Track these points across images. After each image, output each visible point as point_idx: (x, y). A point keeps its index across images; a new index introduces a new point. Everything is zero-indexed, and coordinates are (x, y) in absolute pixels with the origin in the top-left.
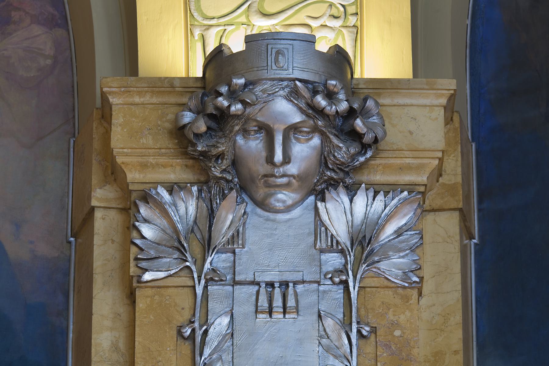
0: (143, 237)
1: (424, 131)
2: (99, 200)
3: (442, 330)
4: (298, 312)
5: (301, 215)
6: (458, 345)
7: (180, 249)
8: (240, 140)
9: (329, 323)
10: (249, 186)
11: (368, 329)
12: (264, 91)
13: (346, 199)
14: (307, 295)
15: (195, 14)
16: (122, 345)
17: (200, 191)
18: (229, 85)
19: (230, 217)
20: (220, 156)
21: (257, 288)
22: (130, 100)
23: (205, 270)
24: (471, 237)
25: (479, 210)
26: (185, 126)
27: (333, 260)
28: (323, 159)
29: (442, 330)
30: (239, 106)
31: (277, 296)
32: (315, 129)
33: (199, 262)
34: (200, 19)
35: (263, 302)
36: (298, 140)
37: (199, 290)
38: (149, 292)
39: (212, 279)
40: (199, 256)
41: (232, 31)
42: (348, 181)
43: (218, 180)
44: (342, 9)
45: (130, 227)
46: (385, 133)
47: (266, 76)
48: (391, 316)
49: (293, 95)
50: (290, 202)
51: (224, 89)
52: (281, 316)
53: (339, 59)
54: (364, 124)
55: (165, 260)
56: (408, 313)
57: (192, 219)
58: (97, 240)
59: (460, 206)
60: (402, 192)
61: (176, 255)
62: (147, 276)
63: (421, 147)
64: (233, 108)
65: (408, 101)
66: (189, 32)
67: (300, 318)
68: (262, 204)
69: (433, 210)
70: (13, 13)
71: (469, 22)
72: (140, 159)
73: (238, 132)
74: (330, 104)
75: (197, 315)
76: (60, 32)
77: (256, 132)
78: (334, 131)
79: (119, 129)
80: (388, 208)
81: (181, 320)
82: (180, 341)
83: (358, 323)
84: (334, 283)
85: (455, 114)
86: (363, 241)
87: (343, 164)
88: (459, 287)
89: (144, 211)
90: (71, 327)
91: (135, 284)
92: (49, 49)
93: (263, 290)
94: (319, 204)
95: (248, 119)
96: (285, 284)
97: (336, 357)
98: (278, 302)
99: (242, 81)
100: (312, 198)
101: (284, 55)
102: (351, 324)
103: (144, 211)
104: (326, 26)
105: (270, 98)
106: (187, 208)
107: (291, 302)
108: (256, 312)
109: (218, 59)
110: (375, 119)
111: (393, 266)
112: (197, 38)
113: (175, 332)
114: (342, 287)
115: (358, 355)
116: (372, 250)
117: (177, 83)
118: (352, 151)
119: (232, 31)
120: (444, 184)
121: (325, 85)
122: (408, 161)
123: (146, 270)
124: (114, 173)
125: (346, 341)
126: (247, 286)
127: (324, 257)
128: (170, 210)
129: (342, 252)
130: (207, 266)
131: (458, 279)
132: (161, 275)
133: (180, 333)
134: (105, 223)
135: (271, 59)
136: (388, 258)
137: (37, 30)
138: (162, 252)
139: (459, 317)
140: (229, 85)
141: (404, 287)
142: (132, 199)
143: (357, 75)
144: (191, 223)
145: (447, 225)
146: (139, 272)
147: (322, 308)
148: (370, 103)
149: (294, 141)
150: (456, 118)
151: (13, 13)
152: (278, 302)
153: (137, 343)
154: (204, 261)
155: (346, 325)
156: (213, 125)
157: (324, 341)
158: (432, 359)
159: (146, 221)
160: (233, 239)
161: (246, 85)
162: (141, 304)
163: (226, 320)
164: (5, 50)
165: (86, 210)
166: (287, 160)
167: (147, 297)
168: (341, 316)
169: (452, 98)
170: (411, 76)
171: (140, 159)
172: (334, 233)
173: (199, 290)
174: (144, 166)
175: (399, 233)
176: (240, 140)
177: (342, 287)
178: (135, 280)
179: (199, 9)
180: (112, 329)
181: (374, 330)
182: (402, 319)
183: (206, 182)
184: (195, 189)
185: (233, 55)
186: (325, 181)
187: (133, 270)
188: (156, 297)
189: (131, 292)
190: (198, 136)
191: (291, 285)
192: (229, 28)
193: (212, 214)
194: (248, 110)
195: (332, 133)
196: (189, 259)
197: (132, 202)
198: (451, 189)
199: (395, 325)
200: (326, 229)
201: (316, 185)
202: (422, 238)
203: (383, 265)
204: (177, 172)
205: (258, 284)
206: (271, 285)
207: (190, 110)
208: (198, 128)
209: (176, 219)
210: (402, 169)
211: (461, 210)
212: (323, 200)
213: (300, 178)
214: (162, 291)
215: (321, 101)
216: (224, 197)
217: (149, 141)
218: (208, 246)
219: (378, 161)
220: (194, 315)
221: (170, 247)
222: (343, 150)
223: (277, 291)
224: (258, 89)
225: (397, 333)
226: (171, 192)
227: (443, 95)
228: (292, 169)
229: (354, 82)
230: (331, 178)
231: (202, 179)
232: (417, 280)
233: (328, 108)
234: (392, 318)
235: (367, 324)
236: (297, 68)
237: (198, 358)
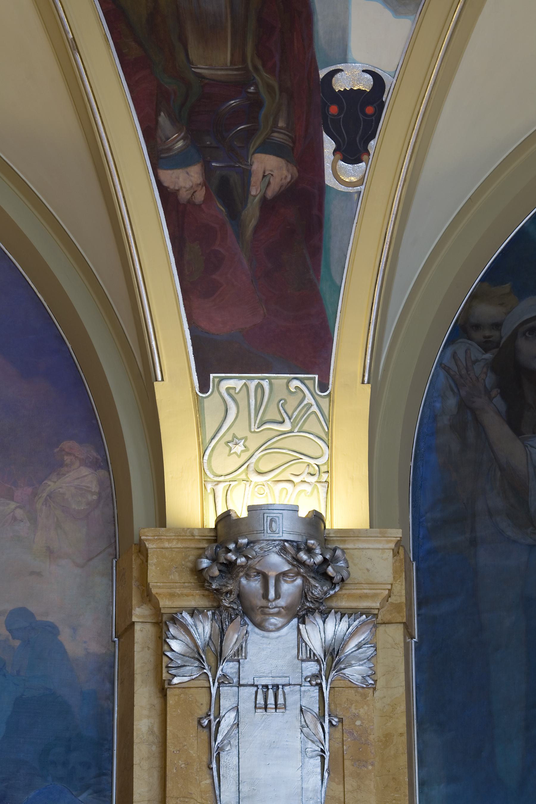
0: (173, 651)
1: (379, 568)
2: (138, 617)
3: (391, 717)
4: (285, 708)
5: (288, 632)
6: (404, 730)
7: (200, 659)
8: (244, 581)
9: (309, 717)
10: (250, 612)
11: (336, 720)
12: (261, 549)
13: (320, 622)
14: (293, 698)
15: (208, 473)
16: (156, 729)
17: (213, 614)
18: (236, 543)
19: (236, 636)
20: (230, 592)
21: (255, 688)
22: (162, 545)
23: (218, 675)
24: (412, 637)
25: (418, 615)
26: (203, 569)
27: (311, 668)
28: (304, 594)
29: (391, 717)
30: (243, 559)
31: (271, 696)
32: (298, 574)
33: (213, 669)
34: (211, 476)
35: (260, 700)
36: (286, 581)
37: (214, 691)
38: (177, 691)
39: (223, 682)
40: (213, 664)
41: (236, 485)
42: (322, 608)
43: (227, 608)
44: (317, 468)
45: (161, 640)
46: (349, 574)
47: (263, 538)
48: (353, 710)
49: (283, 550)
50: (280, 625)
51: (232, 546)
52: (274, 711)
54: (334, 570)
55: (188, 668)
56: (366, 708)
57: (208, 636)
58: (137, 648)
59: (404, 620)
60: (361, 615)
61: (197, 664)
62: (176, 681)
63: (376, 581)
64: (239, 561)
65: (366, 546)
66: (203, 487)
67: (287, 712)
68: (260, 626)
69: (384, 623)
70: (66, 458)
71: (412, 464)
72: (169, 591)
73: (242, 576)
74: (310, 557)
75: (213, 710)
76: (102, 473)
77: (255, 576)
78: (312, 575)
79: (154, 568)
80: (351, 628)
81: (200, 713)
82: (200, 729)
83: (329, 715)
84: (312, 685)
85: (401, 548)
86: (333, 654)
87: (318, 598)
88: (404, 683)
89: (173, 630)
90: (116, 709)
91: (166, 686)
92: (94, 487)
93: (260, 691)
94: (301, 626)
95: (250, 568)
96: (277, 686)
97: (313, 742)
98: (271, 700)
99: (245, 541)
100: (295, 620)
101: (276, 522)
102: (324, 716)
103: (173, 630)
104: (305, 481)
105: (266, 553)
106: (203, 629)
107: (281, 701)
108: (255, 707)
109: (225, 518)
110: (341, 564)
111: (355, 672)
112: (209, 491)
113: (196, 723)
114: (317, 687)
115: (330, 740)
116: (340, 660)
117: (196, 533)
118: (325, 589)
119: (236, 485)
120: (392, 603)
121: (306, 543)
122: (365, 591)
123: (175, 676)
124: (148, 597)
125: (321, 730)
126: (248, 688)
127: (304, 665)
128: (192, 630)
129: (318, 661)
130: (219, 672)
131: (402, 676)
132: (186, 679)
133: (200, 723)
134: (143, 634)
135: (267, 525)
136: (351, 665)
137: (85, 471)
138: (186, 662)
139: (403, 707)
140: (236, 543)
141: (363, 687)
142: (164, 620)
143: (328, 527)
144: (207, 639)
145: (394, 634)
146: (170, 677)
147: (303, 704)
148: (338, 553)
149: (282, 582)
150: (401, 551)
151: (66, 458)
152: (271, 700)
153: (168, 732)
154: (217, 668)
155: (321, 717)
156: (223, 568)
157: (305, 730)
158: (384, 739)
159: (174, 638)
160: (238, 652)
161: (248, 544)
162: (171, 701)
163: (233, 714)
164: (61, 488)
165: (128, 623)
166: (278, 596)
167: (175, 695)
168: (316, 710)
169: (398, 544)
170: (368, 527)
171: (169, 591)
172: (312, 648)
173: (214, 691)
174: (172, 596)
175: (359, 646)
176: (244, 581)
177: (317, 687)
178: (166, 683)
179: (210, 469)
180: (149, 717)
181: (341, 720)
182: (362, 711)
183: (218, 608)
184: (210, 613)
185: (239, 520)
186: (306, 609)
187: (165, 676)
188: (182, 696)
189: (163, 689)
190: (213, 578)
191: (280, 687)
192: (233, 484)
193: (222, 632)
194: (250, 562)
195: (310, 576)
196: (207, 667)
197: (163, 623)
198: (397, 607)
199: (356, 717)
200: (306, 644)
201: (298, 611)
202: (376, 650)
203: (347, 671)
204: (196, 600)
205: (257, 686)
206: (266, 686)
207: (207, 558)
208: (213, 573)
209: (196, 636)
210: (361, 597)
211: (404, 623)
212: (304, 623)
213: (286, 608)
214: (187, 690)
215: (303, 556)
216: (232, 620)
217: (175, 577)
218: (219, 657)
219: (344, 592)
220: (210, 710)
221: (192, 658)
222: (318, 589)
223: (271, 692)
224: (257, 547)
225: (358, 723)
226: (192, 615)
227: (391, 541)
228: (282, 602)
229: (326, 532)
230: (310, 608)
231: (215, 604)
232: (373, 682)
233: (309, 561)
234: (354, 711)
235: (336, 716)
236: (286, 530)
237: (213, 743)
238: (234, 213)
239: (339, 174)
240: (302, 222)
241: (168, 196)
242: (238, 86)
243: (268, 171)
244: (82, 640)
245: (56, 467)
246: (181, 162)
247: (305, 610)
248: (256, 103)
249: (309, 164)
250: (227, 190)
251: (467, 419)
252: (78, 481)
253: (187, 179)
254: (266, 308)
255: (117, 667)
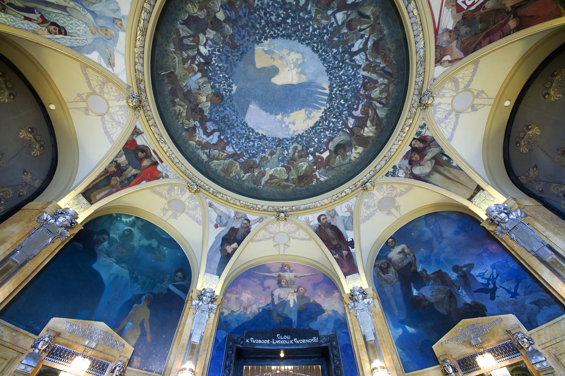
53: (361, 288)
86: (368, 303)
111: (372, 305)
124: (346, 303)
134: (346, 308)
204: (351, 301)
222: (364, 295)
236: (358, 289)
238: (343, 258)
239: (352, 250)
240: (350, 256)
241: (335, 258)
242: (338, 244)
243: (345, 252)
244: (341, 312)
245: (334, 293)
246: (335, 254)
247: (364, 298)
248: (341, 246)
249: (349, 250)
250: (341, 256)
251: (378, 275)
252: (336, 294)
253: (337, 256)
254: (350, 268)
255: (345, 314)
